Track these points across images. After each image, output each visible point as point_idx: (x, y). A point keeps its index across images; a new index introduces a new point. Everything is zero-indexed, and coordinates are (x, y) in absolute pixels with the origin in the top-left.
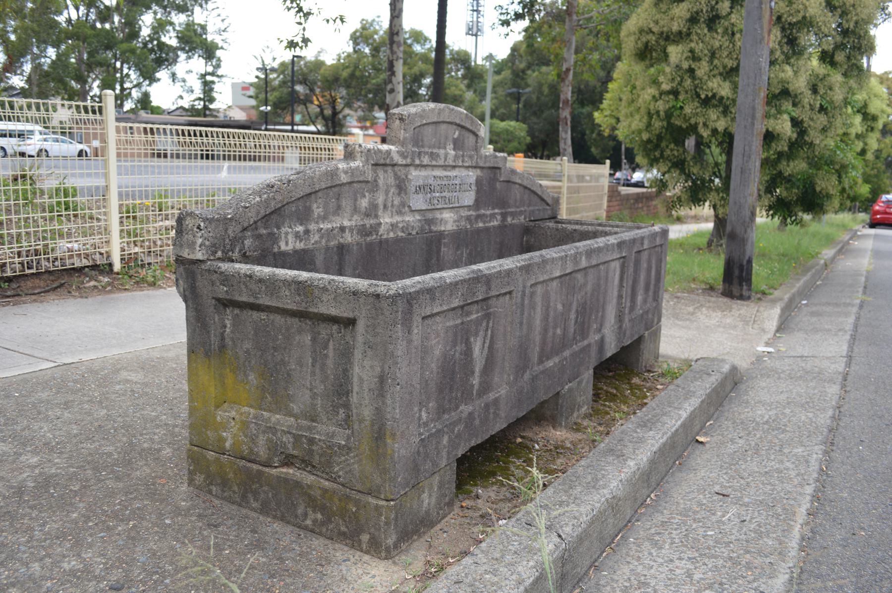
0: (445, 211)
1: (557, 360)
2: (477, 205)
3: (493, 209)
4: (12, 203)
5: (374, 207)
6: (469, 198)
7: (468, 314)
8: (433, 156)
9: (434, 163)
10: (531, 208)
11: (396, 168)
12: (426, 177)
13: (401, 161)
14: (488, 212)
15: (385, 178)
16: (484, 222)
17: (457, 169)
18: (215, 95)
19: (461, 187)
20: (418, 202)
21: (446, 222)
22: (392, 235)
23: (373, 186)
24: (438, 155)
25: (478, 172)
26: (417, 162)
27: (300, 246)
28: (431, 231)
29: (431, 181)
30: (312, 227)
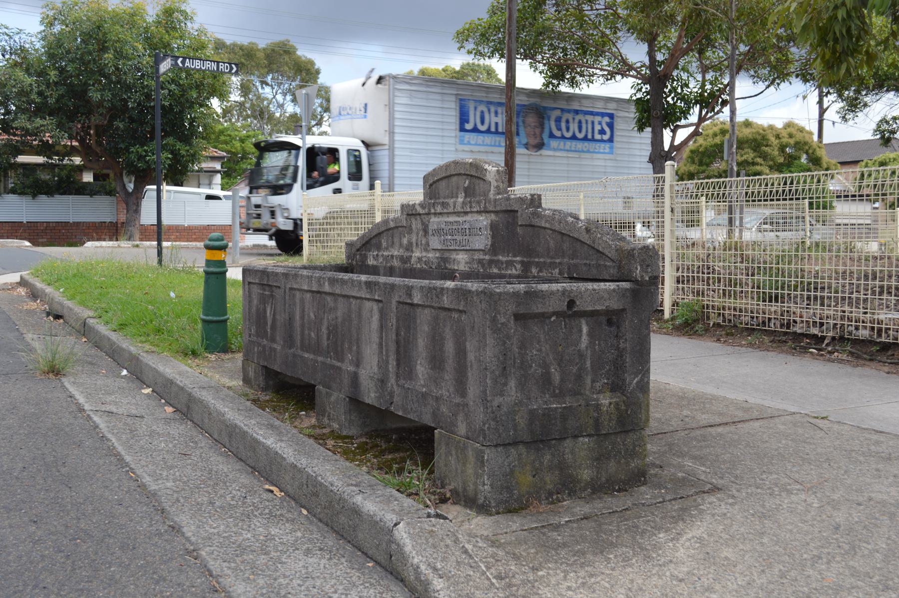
0: (461, 253)
1: (312, 356)
2: (494, 249)
3: (515, 256)
4: (862, 282)
5: (410, 243)
6: (482, 242)
7: (264, 290)
8: (444, 205)
9: (445, 211)
10: (575, 261)
11: (422, 217)
12: (439, 223)
13: (421, 211)
14: (505, 259)
15: (416, 224)
16: (499, 270)
17: (470, 215)
18: (650, 166)
19: (472, 231)
20: (435, 243)
21: (459, 263)
22: (419, 266)
23: (410, 230)
24: (448, 204)
25: (493, 216)
26: (433, 211)
27: (375, 263)
28: (446, 268)
29: (443, 226)
30: (380, 254)
